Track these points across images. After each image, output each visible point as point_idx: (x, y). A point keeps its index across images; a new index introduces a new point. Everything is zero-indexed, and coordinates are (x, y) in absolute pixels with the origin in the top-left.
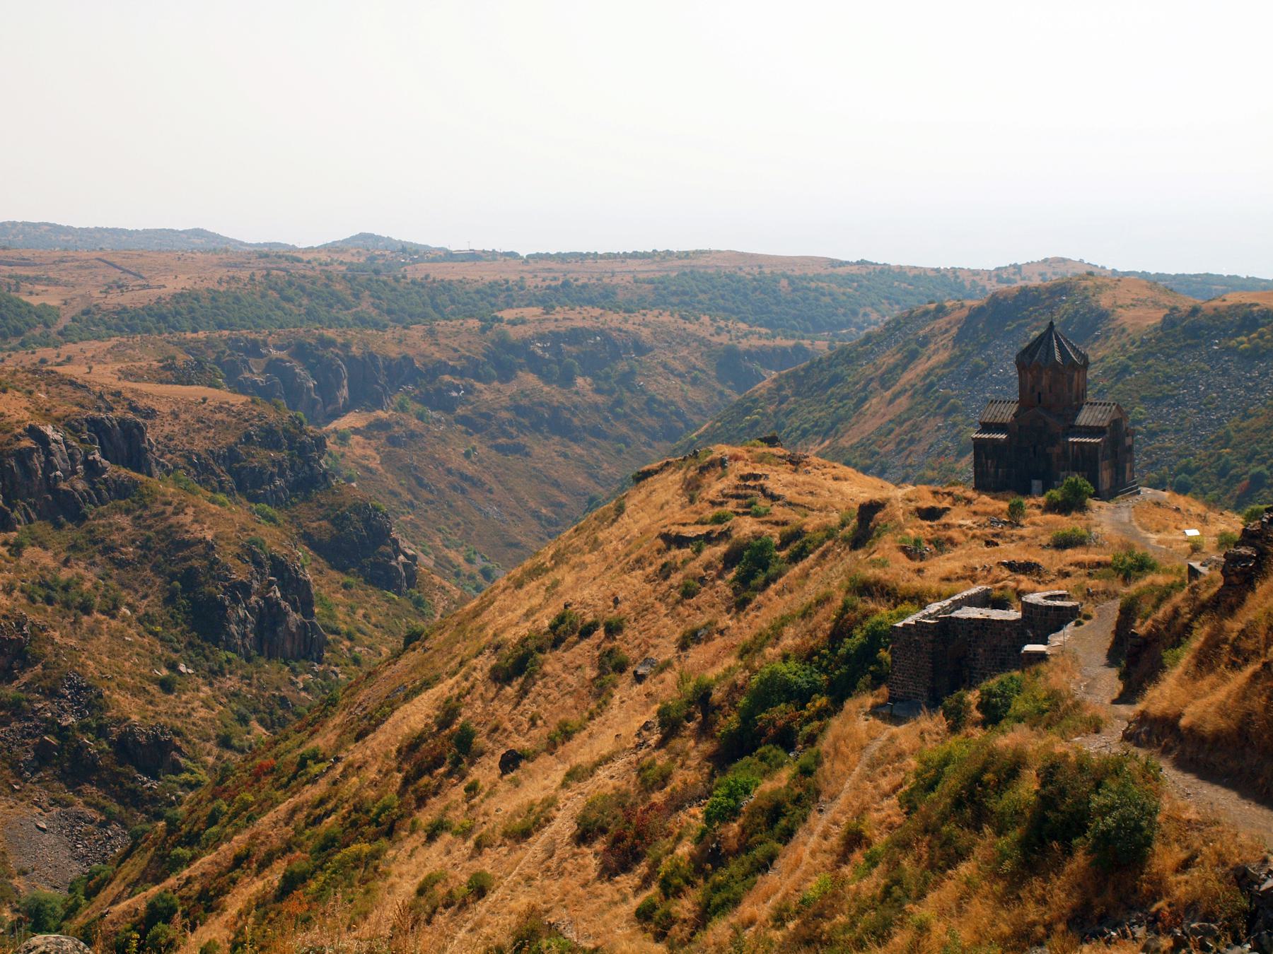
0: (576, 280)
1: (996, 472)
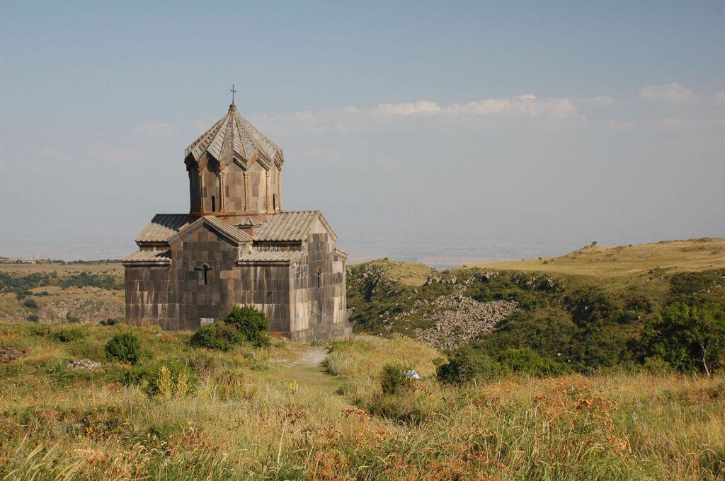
0: (90, 273)
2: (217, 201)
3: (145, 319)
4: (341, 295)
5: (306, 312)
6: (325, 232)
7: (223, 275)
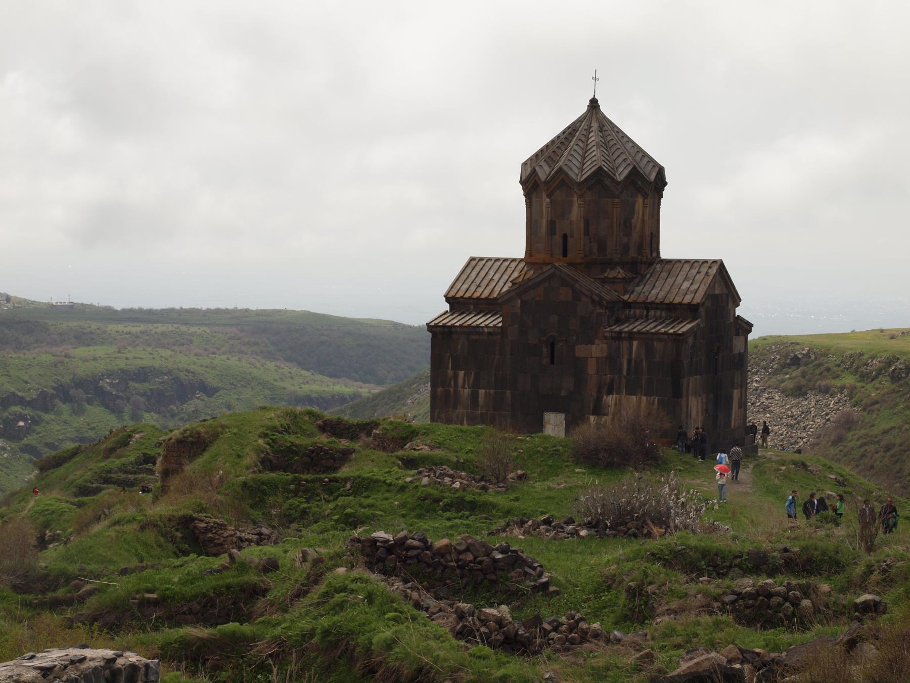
1: (474, 397)
2: (569, 239)
3: (460, 410)
4: (741, 387)
5: (700, 410)
6: (726, 292)
7: (581, 351)
